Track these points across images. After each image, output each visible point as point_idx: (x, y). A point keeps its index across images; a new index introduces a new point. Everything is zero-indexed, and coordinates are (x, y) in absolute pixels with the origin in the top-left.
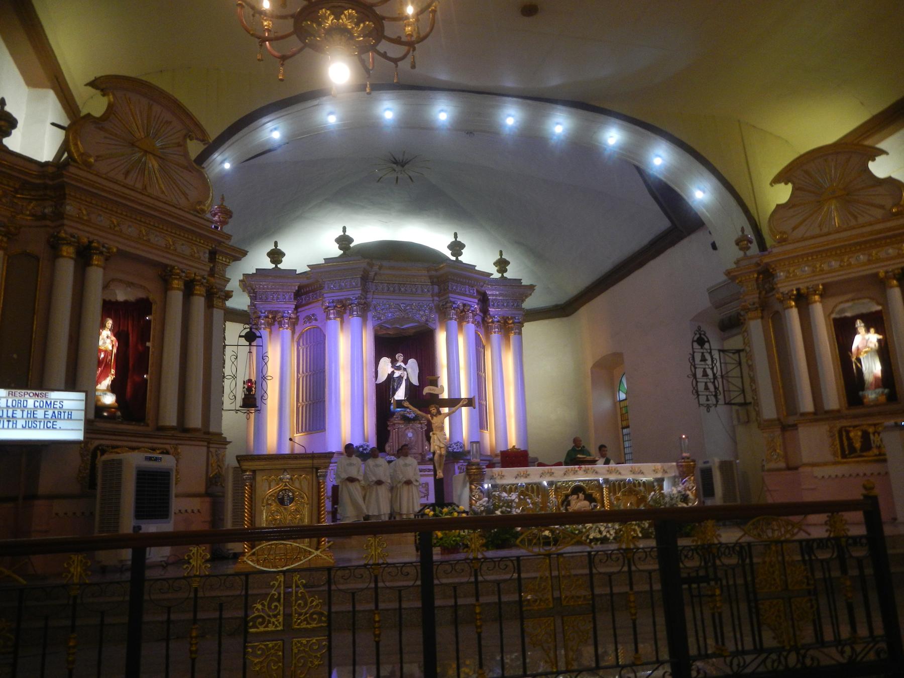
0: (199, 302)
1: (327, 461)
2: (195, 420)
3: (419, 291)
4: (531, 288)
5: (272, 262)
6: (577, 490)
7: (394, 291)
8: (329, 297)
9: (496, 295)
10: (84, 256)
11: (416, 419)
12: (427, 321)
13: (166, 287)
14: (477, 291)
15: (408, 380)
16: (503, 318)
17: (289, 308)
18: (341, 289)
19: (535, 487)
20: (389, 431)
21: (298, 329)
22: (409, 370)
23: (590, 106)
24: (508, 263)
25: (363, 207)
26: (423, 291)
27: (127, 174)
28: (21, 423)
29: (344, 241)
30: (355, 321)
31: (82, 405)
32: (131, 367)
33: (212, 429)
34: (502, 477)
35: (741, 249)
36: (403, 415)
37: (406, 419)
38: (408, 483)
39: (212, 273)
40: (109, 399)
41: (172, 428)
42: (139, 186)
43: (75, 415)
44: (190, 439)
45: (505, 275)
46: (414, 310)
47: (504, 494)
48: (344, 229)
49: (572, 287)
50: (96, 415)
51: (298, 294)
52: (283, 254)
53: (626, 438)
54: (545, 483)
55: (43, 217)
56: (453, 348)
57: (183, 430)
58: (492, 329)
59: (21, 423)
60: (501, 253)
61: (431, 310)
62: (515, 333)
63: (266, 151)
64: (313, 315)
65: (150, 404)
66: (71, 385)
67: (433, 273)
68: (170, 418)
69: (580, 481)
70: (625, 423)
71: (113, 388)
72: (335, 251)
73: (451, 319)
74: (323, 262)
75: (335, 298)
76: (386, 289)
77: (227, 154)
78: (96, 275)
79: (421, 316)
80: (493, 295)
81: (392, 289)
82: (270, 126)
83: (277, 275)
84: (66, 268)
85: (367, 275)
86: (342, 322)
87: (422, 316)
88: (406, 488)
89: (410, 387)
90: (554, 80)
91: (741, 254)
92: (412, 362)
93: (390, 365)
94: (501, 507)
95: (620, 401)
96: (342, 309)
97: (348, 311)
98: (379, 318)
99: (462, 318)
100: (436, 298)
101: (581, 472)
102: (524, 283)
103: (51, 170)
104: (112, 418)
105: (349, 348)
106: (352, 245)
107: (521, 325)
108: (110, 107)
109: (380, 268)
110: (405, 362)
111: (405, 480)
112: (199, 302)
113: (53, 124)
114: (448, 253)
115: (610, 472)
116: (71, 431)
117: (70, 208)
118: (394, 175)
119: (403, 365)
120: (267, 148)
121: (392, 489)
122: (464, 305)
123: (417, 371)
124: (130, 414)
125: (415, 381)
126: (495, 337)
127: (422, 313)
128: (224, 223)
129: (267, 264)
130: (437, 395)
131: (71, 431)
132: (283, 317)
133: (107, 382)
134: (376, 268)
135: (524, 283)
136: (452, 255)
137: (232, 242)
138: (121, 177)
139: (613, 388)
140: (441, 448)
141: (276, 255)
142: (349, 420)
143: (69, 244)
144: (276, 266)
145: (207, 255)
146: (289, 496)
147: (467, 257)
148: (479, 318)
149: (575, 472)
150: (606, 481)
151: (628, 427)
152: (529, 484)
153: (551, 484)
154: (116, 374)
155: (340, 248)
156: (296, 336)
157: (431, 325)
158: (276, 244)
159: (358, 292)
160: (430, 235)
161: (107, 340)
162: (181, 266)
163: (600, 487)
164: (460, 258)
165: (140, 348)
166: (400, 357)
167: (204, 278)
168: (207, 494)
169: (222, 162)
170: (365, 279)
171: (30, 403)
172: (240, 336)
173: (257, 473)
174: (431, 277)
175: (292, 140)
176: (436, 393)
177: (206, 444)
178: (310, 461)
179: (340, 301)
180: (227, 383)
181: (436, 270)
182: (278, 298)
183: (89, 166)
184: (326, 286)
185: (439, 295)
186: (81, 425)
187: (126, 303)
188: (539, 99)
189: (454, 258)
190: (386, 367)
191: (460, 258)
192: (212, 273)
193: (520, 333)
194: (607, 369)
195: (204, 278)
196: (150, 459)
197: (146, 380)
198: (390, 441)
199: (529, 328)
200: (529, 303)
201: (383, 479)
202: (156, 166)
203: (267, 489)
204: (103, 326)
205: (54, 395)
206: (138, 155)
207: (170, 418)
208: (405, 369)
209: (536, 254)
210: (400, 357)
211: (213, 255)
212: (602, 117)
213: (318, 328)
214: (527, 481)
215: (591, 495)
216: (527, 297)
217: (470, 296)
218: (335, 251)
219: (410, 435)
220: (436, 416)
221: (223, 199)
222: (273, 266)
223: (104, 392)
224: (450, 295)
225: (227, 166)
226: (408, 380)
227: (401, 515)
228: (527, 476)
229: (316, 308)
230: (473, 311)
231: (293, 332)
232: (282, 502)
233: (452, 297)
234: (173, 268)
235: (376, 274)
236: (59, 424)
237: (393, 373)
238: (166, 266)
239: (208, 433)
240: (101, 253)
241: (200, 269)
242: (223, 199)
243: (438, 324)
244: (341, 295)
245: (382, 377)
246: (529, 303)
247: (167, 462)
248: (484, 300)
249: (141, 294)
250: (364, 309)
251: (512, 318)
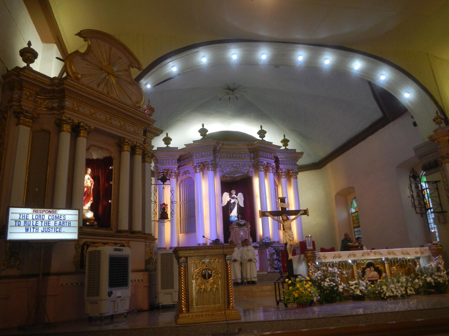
0: (138, 158)
1: (232, 250)
2: (138, 227)
3: (243, 157)
4: (302, 153)
5: (165, 144)
6: (370, 265)
7: (230, 157)
8: (196, 160)
9: (283, 158)
10: (76, 130)
11: (244, 225)
12: (248, 172)
13: (121, 149)
14: (274, 157)
15: (238, 204)
16: (287, 170)
17: (175, 167)
18: (202, 156)
19: (344, 263)
20: (230, 232)
21: (180, 179)
22: (239, 199)
23: (345, 48)
24: (288, 141)
25: (212, 114)
26: (245, 157)
27: (98, 85)
28: (41, 229)
29: (203, 131)
30: (211, 173)
31: (76, 218)
33: (147, 232)
34: (325, 258)
35: (437, 124)
36: (239, 224)
37: (239, 225)
38: (250, 260)
39: (145, 142)
40: (90, 215)
41: (126, 231)
42: (105, 92)
43: (73, 224)
44: (136, 237)
45: (287, 147)
46: (242, 166)
47: (330, 269)
48: (203, 125)
49: (323, 154)
50: (84, 224)
51: (179, 160)
52: (171, 140)
53: (356, 233)
54: (350, 261)
55: (53, 109)
57: (131, 231)
58: (281, 176)
59: (41, 229)
60: (284, 136)
61: (250, 166)
62: (294, 178)
63: (169, 79)
64: (188, 171)
65: (113, 217)
66: (69, 206)
67: (250, 147)
68: (124, 226)
69: (371, 259)
70: (355, 225)
71: (92, 208)
72: (198, 137)
73: (261, 171)
74: (192, 142)
75: (199, 161)
76: (226, 155)
77: (148, 80)
78: (82, 142)
79: (245, 170)
80: (281, 158)
81: (229, 156)
82: (171, 64)
83: (168, 150)
84: (66, 138)
85: (216, 148)
86: (203, 174)
87: (245, 170)
88: (249, 264)
89: (239, 208)
90: (323, 34)
91: (437, 126)
92: (240, 194)
93: (229, 196)
94: (328, 277)
95: (352, 213)
96: (203, 167)
97: (206, 168)
98: (223, 171)
99: (266, 171)
100: (253, 160)
101: (372, 254)
102: (297, 151)
103: (57, 81)
104: (92, 225)
106: (207, 133)
107: (297, 173)
108: (89, 47)
109: (223, 145)
110: (237, 194)
111: (248, 259)
112: (138, 158)
113: (57, 58)
114: (257, 137)
115: (389, 253)
116: (70, 234)
117: (68, 103)
118: (228, 96)
119: (235, 196)
120: (169, 77)
121: (241, 264)
122: (268, 163)
123: (243, 199)
125: (242, 205)
126: (283, 180)
127: (245, 168)
128: (150, 115)
129: (162, 145)
130: (285, 208)
131: (70, 234)
132: (172, 172)
133: (88, 205)
134: (220, 145)
135: (297, 151)
136: (260, 137)
137: (155, 125)
138: (95, 87)
139: (348, 206)
140: (290, 240)
141: (167, 140)
143: (68, 123)
144: (168, 146)
145: (142, 132)
146: (209, 273)
147: (267, 138)
148: (274, 171)
149: (369, 254)
150: (387, 259)
151: (359, 227)
152: (340, 262)
153: (354, 261)
154: (93, 200)
155: (201, 135)
156: (179, 183)
157: (250, 174)
158: (167, 134)
159: (212, 158)
160: (249, 128)
161: (88, 181)
162: (129, 138)
163: (383, 263)
164: (264, 139)
165: (106, 185)
166: (233, 192)
167: (141, 145)
168: (146, 270)
169: (146, 84)
170: (215, 151)
171: (46, 217)
172: (158, 179)
173: (189, 259)
174: (249, 149)
175: (183, 73)
176: (285, 207)
177: (144, 240)
178: (222, 251)
179: (202, 163)
180: (152, 205)
181: (252, 145)
182: (169, 163)
183: (77, 79)
184: (195, 155)
185: (254, 158)
186: (76, 230)
187: (98, 160)
188: (318, 45)
189: (261, 139)
190: (226, 197)
191: (264, 139)
192: (145, 142)
193: (296, 178)
194: (344, 196)
195: (141, 145)
196: (116, 250)
197: (110, 203)
198: (231, 237)
199: (301, 175)
200: (301, 162)
201: (237, 259)
202: (114, 82)
203: (194, 269)
204: (86, 173)
205: (61, 212)
206: (105, 75)
207: (124, 226)
208: (236, 199)
209: (303, 136)
210: (233, 192)
211: (145, 132)
212: (351, 54)
213: (190, 177)
214: (340, 260)
215: (378, 268)
216: (299, 159)
217: (271, 159)
218: (198, 137)
219: (242, 233)
220: (286, 221)
221: (149, 102)
222: (166, 146)
223: (87, 211)
224: (260, 158)
225: (149, 86)
226: (238, 204)
227: (247, 279)
228: (340, 257)
229: (189, 167)
230: (272, 167)
231: (177, 181)
232: (204, 276)
233: (261, 159)
234: (125, 138)
235: (220, 148)
236: (63, 229)
237: (230, 200)
238: (120, 137)
239: (145, 234)
240: (86, 129)
241: (139, 139)
242: (149, 102)
243: (254, 173)
244: (203, 160)
245: (225, 203)
246: (301, 162)
247: (126, 251)
248: (277, 161)
249: (106, 154)
250: (215, 167)
251: (292, 170)
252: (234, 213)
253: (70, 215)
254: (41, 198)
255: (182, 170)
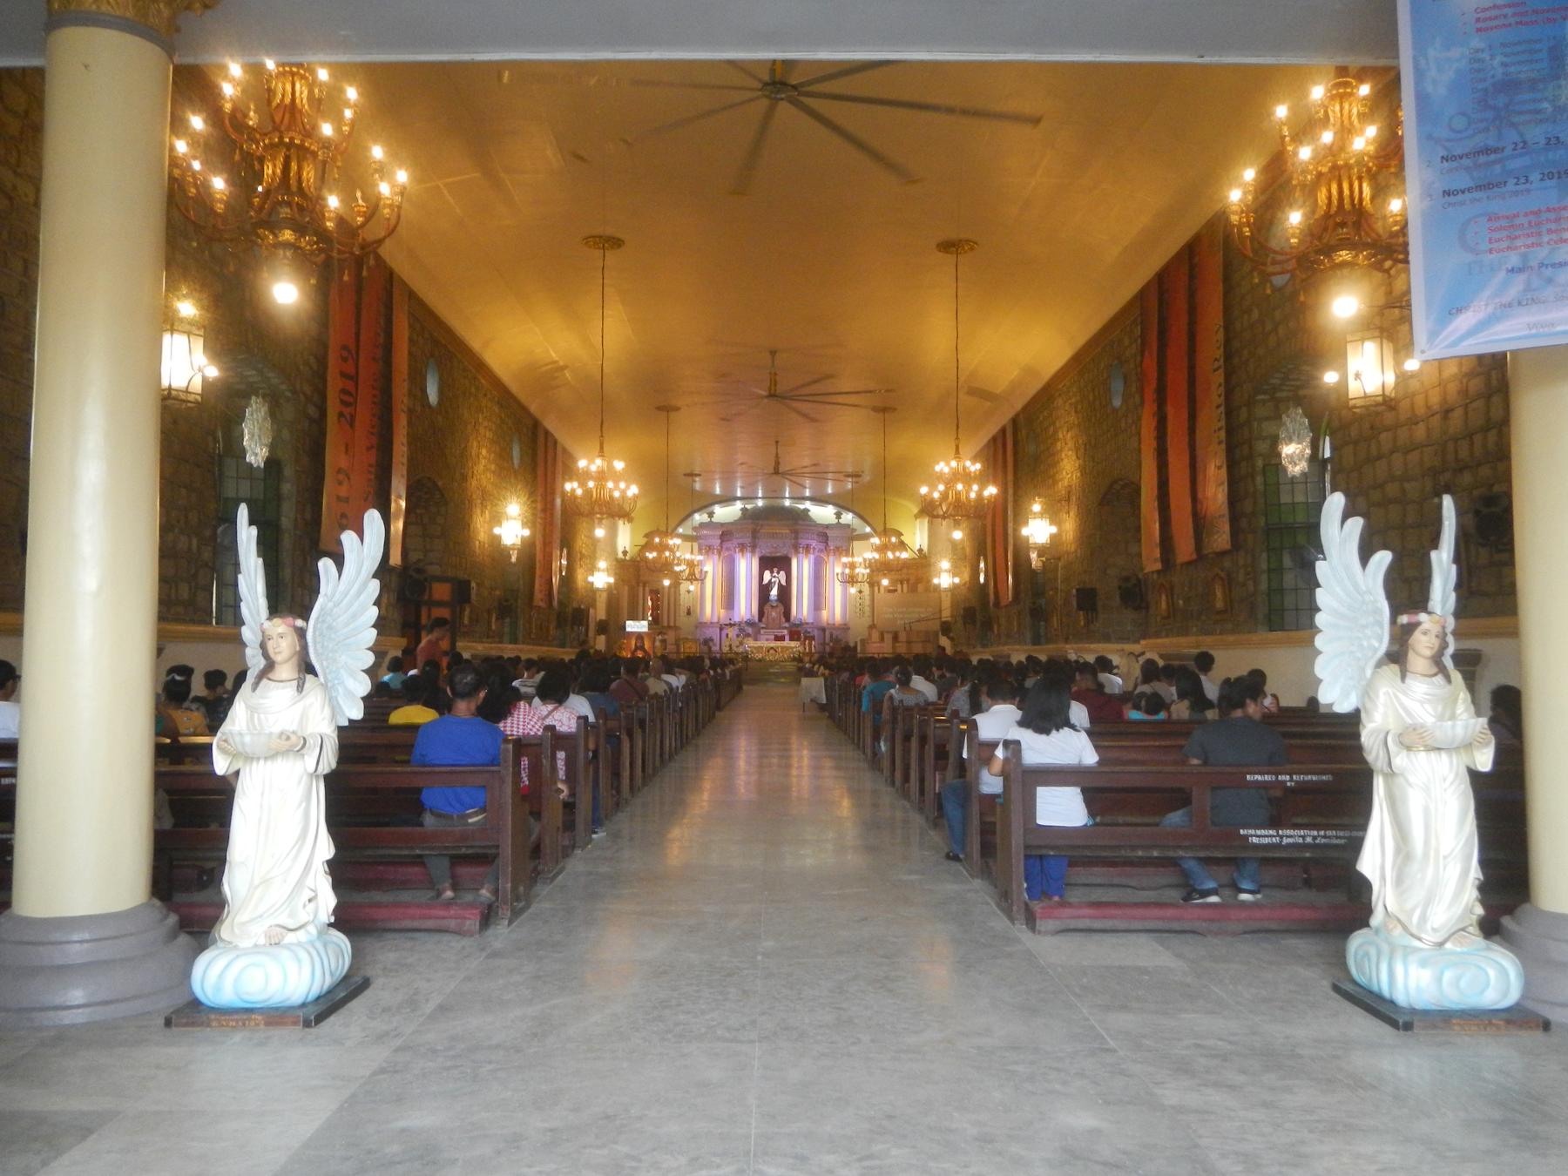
8: (735, 542)
32: (655, 608)
56: (802, 567)
83: (709, 525)
89: (780, 585)
96: (742, 548)
105: (746, 567)
124: (655, 621)
131: (645, 629)
142: (746, 606)
190: (767, 576)
245: (766, 581)
250: (754, 548)
252: (774, 592)
253: (645, 623)
254: (634, 618)
255: (726, 545)
